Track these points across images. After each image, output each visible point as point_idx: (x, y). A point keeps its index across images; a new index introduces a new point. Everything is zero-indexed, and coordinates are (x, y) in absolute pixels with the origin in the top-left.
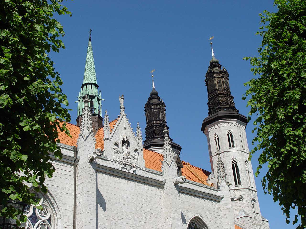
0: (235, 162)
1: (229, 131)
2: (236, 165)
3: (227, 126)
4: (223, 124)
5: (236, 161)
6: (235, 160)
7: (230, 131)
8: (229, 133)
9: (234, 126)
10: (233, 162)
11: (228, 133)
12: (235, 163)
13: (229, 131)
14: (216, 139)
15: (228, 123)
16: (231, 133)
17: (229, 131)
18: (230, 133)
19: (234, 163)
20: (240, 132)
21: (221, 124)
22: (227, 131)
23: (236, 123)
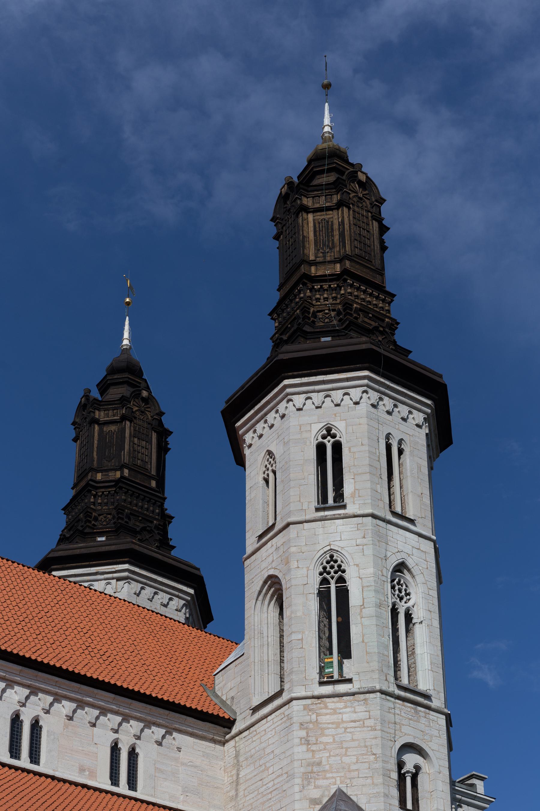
0: (336, 568)
1: (329, 432)
2: (341, 580)
3: (317, 408)
4: (299, 400)
5: (339, 566)
6: (339, 562)
7: (333, 431)
8: (325, 441)
9: (357, 403)
10: (325, 568)
11: (320, 440)
12: (336, 576)
14: (268, 475)
15: (322, 394)
16: (337, 438)
17: (329, 430)
19: (329, 573)
20: (388, 436)
21: (291, 400)
22: (314, 432)
23: (364, 392)
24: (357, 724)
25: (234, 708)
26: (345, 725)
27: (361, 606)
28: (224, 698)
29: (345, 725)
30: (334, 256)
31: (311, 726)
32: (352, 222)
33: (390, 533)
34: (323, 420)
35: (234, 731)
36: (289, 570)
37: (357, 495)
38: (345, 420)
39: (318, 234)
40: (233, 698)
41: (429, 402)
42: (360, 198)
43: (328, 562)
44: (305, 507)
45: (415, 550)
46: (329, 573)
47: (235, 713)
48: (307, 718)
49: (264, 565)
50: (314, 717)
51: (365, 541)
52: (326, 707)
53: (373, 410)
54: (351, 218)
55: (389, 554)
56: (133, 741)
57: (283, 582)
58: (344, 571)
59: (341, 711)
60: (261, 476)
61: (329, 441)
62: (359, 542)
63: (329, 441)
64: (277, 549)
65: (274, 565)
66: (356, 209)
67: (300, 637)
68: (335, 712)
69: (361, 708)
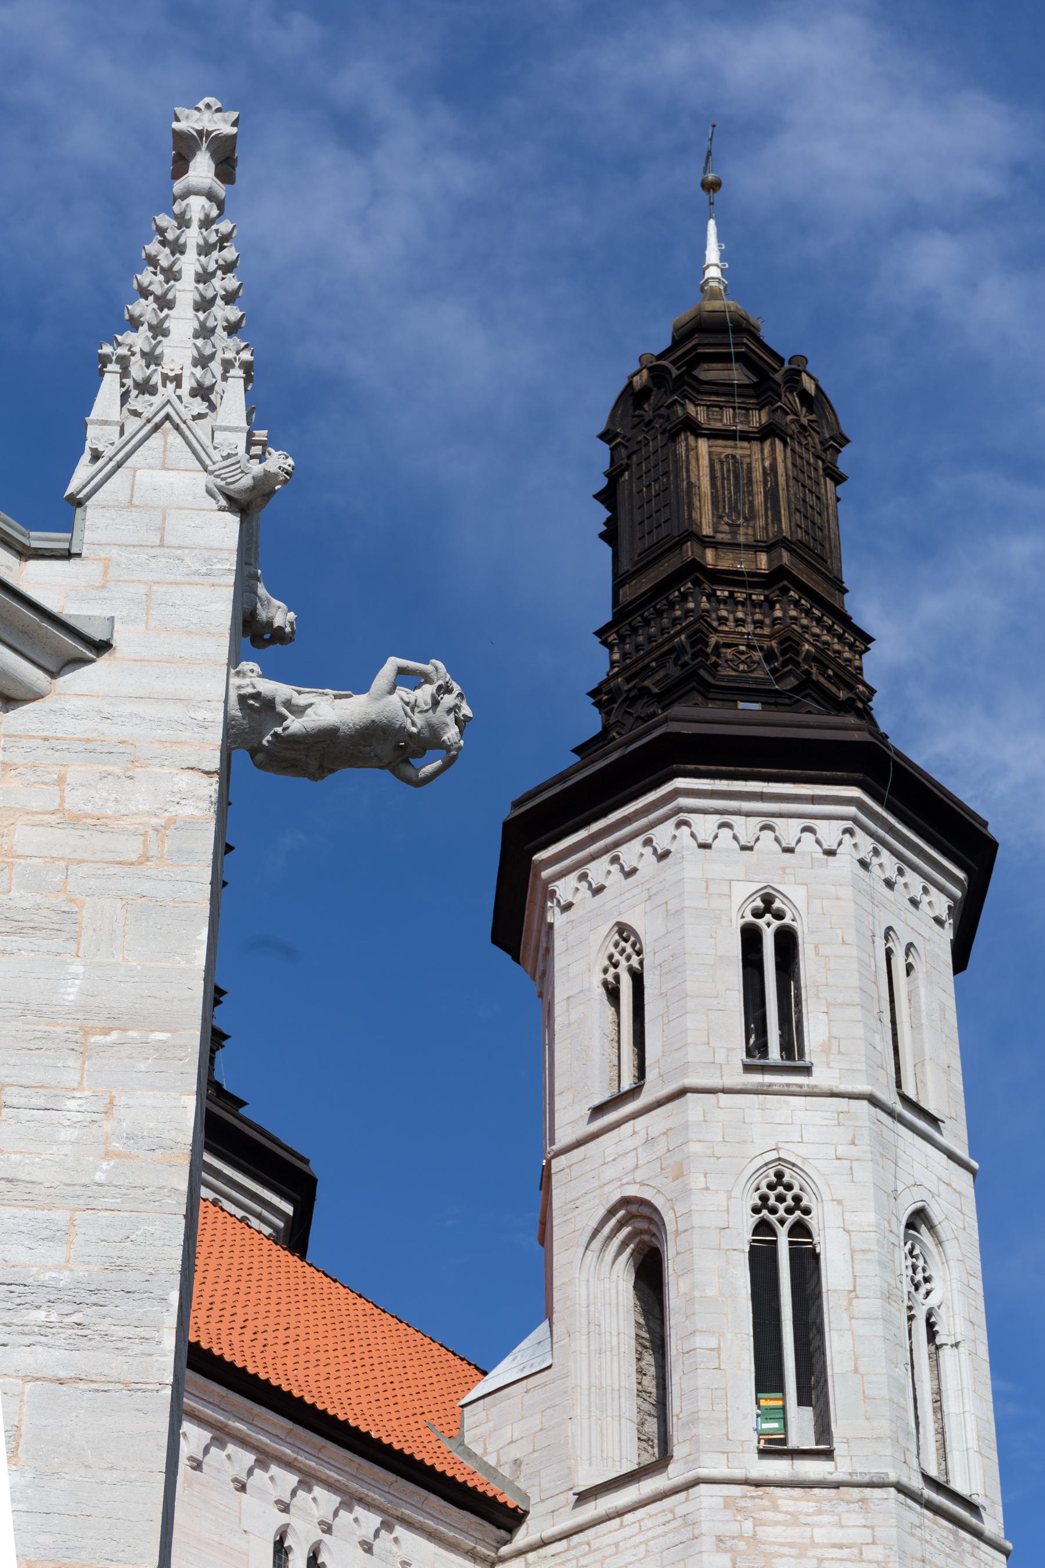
0: (790, 1202)
1: (768, 904)
2: (800, 1229)
3: (744, 848)
4: (705, 826)
5: (797, 1199)
6: (796, 1190)
7: (777, 904)
8: (761, 922)
10: (764, 1198)
12: (791, 1219)
13: (759, 903)
14: (617, 977)
15: (756, 822)
16: (787, 921)
17: (768, 900)
18: (776, 923)
19: (773, 1211)
21: (686, 823)
23: (848, 831)
24: (845, 1553)
25: (521, 1484)
26: (819, 1552)
27: (850, 1292)
28: (492, 1461)
29: (819, 1552)
30: (755, 535)
31: (742, 1545)
32: (790, 473)
33: (901, 1143)
34: (758, 878)
35: (523, 1537)
36: (686, 1192)
37: (835, 1050)
38: (806, 885)
39: (719, 484)
40: (517, 1463)
41: (961, 875)
42: (802, 426)
43: (771, 1187)
44: (720, 1058)
45: (943, 1186)
46: (773, 1211)
47: (526, 1498)
48: (733, 1528)
49: (608, 1173)
50: (748, 1525)
51: (854, 1151)
52: (776, 1508)
53: (861, 871)
54: (790, 465)
55: (900, 1187)
56: (318, 1534)
57: (668, 1217)
58: (807, 1211)
59: (809, 1520)
60: (598, 977)
61: (769, 925)
62: (841, 1151)
63: (769, 925)
64: (649, 1141)
65: (639, 1175)
66: (797, 448)
67: (713, 1343)
68: (794, 1520)
69: (854, 1518)
